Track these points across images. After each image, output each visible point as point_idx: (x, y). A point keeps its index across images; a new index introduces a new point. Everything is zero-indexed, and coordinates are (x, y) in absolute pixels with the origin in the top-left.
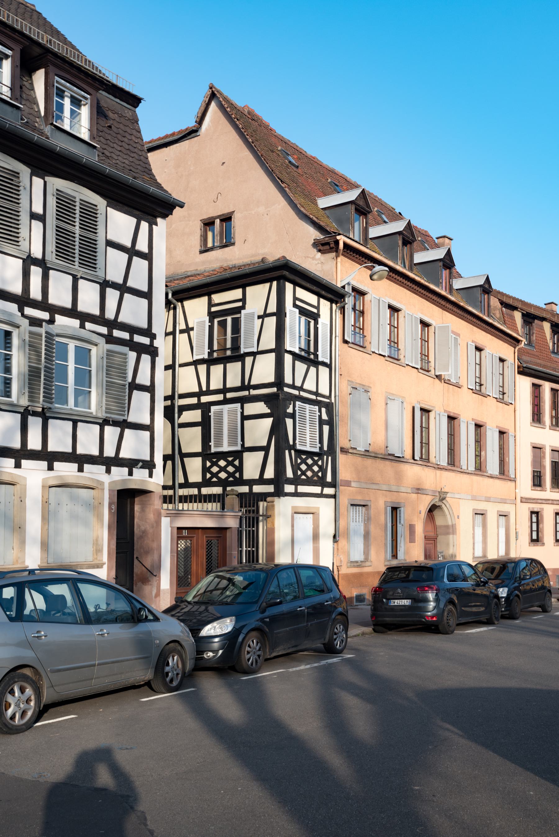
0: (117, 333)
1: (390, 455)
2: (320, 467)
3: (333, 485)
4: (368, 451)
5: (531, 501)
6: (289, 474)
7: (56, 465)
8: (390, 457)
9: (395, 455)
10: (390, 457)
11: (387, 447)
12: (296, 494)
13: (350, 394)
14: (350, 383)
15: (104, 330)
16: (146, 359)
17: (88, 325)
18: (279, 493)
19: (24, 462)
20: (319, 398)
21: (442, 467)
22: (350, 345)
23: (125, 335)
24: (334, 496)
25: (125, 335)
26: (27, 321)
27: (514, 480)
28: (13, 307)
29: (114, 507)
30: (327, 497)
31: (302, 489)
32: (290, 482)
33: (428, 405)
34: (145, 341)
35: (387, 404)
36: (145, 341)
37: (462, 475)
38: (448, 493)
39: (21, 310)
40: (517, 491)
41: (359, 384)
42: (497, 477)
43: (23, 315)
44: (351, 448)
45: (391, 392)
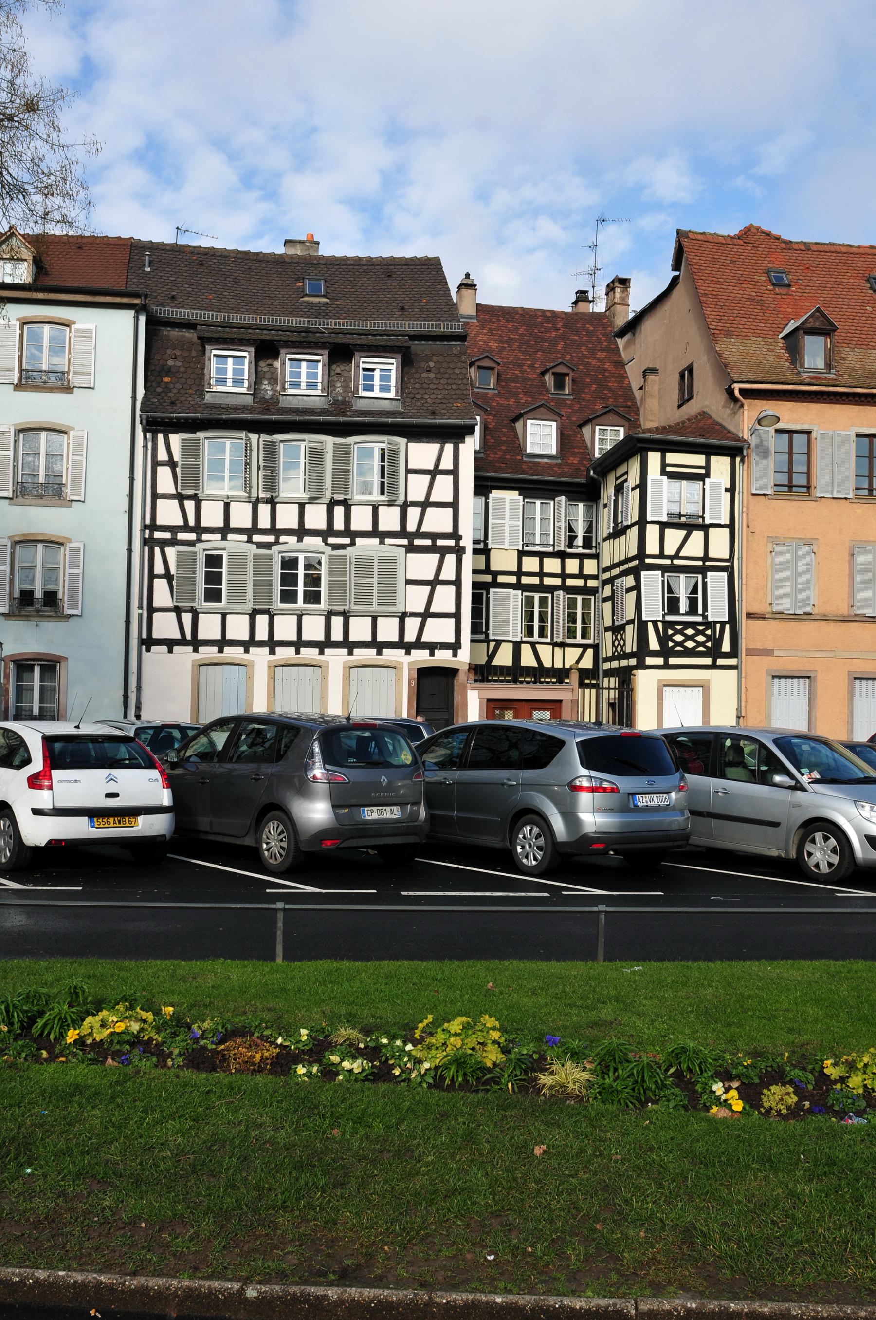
0: (417, 542)
1: (856, 615)
2: (709, 638)
3: (734, 653)
4: (811, 614)
6: (654, 645)
7: (356, 651)
8: (857, 618)
10: (857, 618)
12: (666, 666)
14: (771, 539)
15: (405, 542)
16: (450, 559)
17: (388, 541)
18: (641, 665)
19: (326, 651)
20: (707, 563)
23: (428, 542)
25: (428, 542)
26: (330, 548)
28: (318, 540)
29: (414, 683)
31: (673, 661)
32: (655, 654)
34: (451, 543)
35: (853, 555)
36: (451, 543)
39: (325, 541)
43: (326, 544)
44: (773, 613)
45: (864, 539)
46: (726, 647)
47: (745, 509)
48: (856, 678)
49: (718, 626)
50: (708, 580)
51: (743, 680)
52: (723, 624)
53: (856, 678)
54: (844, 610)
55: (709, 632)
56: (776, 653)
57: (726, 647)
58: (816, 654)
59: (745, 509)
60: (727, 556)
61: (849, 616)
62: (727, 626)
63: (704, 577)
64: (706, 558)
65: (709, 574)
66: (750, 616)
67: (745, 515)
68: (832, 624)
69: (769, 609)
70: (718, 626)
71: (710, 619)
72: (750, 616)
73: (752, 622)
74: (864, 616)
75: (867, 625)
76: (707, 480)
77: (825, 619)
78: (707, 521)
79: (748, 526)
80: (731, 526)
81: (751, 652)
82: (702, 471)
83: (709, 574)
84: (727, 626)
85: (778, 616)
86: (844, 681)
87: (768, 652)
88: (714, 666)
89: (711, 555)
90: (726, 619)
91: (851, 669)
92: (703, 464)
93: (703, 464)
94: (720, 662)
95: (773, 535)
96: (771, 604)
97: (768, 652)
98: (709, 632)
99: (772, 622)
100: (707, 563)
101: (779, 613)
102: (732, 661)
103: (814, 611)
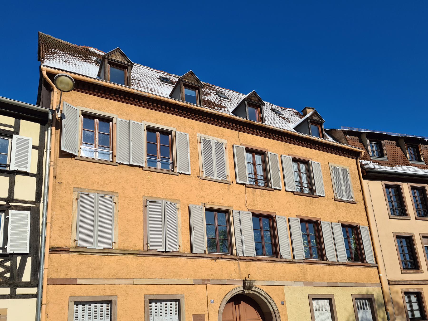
1: (149, 250)
5: (403, 283)
8: (151, 253)
9: (158, 250)
11: (147, 244)
13: (77, 199)
14: (77, 189)
20: (11, 204)
21: (246, 258)
22: (76, 158)
24: (35, 296)
27: (376, 265)
30: (20, 298)
33: (218, 206)
35: (146, 206)
37: (284, 264)
38: (255, 281)
40: (381, 275)
41: (94, 190)
42: (344, 263)
44: (77, 247)
46: (27, 277)
47: (52, 163)
48: (151, 301)
49: (19, 258)
50: (10, 217)
51: (44, 307)
52: (24, 256)
53: (151, 301)
54: (140, 246)
55: (8, 264)
56: (79, 282)
57: (27, 277)
58: (117, 282)
59: (52, 163)
60: (33, 199)
61: (144, 251)
62: (29, 259)
63: (7, 214)
64: (10, 198)
65: (11, 212)
66: (53, 250)
67: (52, 168)
68: (130, 258)
69: (73, 244)
70: (19, 258)
71: (9, 251)
72: (53, 250)
73: (56, 256)
74: (156, 251)
75: (159, 258)
76: (14, 136)
77: (124, 253)
78: (13, 168)
79: (55, 177)
80: (39, 176)
81: (52, 282)
82: (12, 130)
83: (11, 212)
84: (29, 259)
85: (81, 250)
86: (141, 304)
87: (72, 281)
88: (13, 296)
89: (16, 197)
90: (28, 252)
91: (146, 293)
92: (13, 124)
93: (13, 124)
94: (20, 291)
95: (79, 187)
96: (75, 241)
97: (72, 281)
98: (8, 264)
99: (76, 255)
100: (11, 204)
101: (82, 247)
102: (33, 291)
103: (116, 246)
